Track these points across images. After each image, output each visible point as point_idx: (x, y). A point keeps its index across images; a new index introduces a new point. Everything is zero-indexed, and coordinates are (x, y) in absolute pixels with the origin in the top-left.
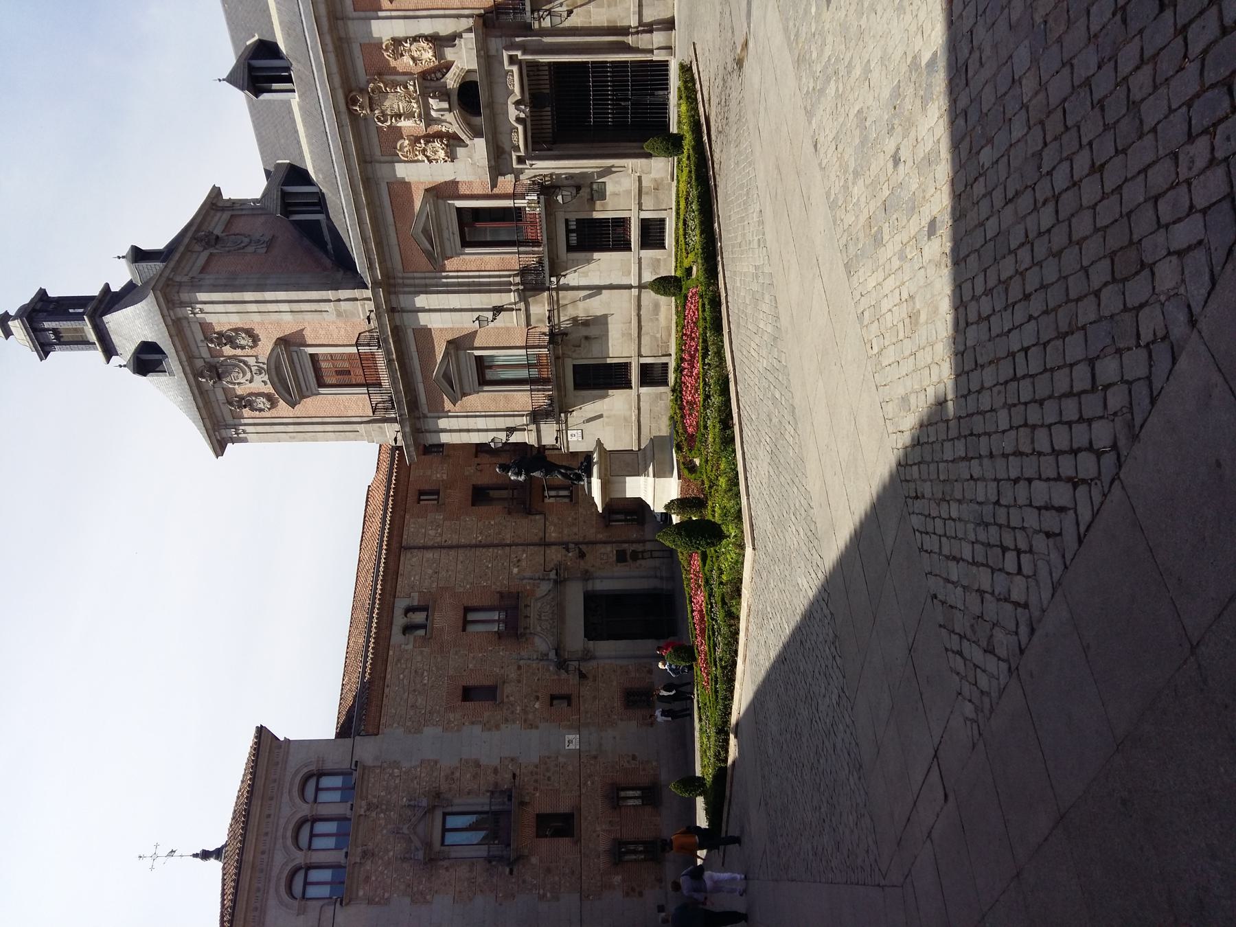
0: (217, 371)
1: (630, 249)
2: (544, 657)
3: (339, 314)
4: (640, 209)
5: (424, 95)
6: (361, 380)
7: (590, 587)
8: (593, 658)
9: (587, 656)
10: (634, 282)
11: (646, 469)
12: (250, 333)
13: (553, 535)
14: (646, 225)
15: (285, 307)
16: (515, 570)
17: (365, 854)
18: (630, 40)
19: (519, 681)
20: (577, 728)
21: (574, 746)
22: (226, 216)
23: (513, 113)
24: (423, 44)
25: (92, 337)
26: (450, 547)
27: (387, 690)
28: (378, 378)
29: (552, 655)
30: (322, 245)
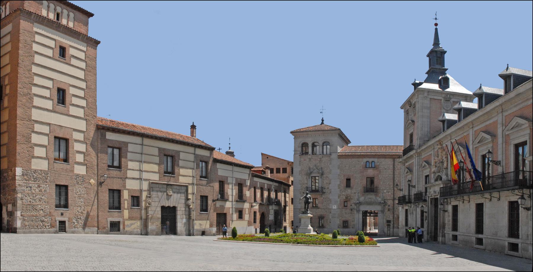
9: (358, 211)
17: (310, 159)
21: (334, 208)
29: (358, 202)
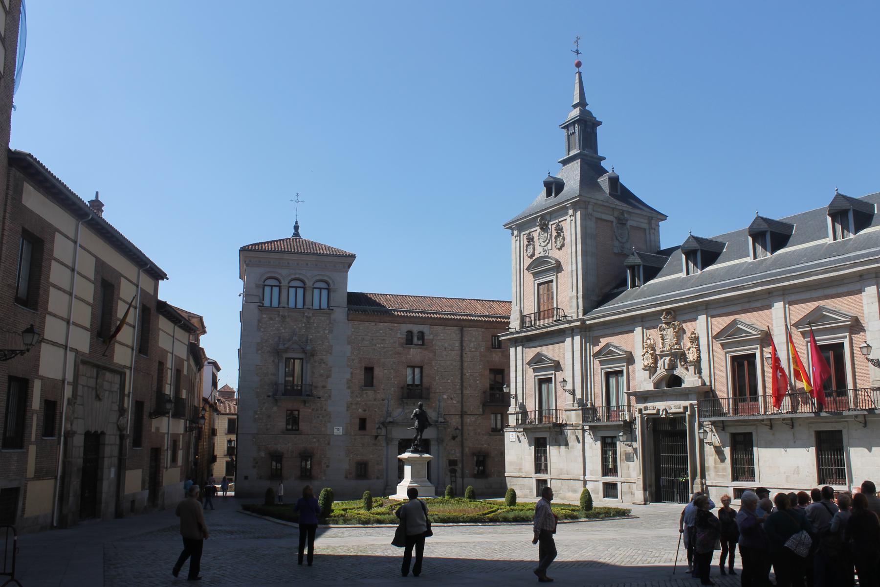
0: (544, 228)
1: (603, 476)
2: (389, 414)
3: (571, 298)
5: (673, 355)
6: (541, 309)
7: (432, 443)
8: (388, 444)
9: (388, 440)
10: (587, 478)
11: (416, 482)
12: (563, 245)
13: (468, 420)
14: (614, 486)
15: (574, 268)
16: (445, 397)
17: (284, 317)
18: (698, 480)
19: (375, 400)
20: (346, 433)
21: (336, 432)
22: (645, 226)
24: (695, 357)
25: (572, 154)
26: (462, 356)
27: (373, 324)
28: (543, 319)
30: (617, 287)
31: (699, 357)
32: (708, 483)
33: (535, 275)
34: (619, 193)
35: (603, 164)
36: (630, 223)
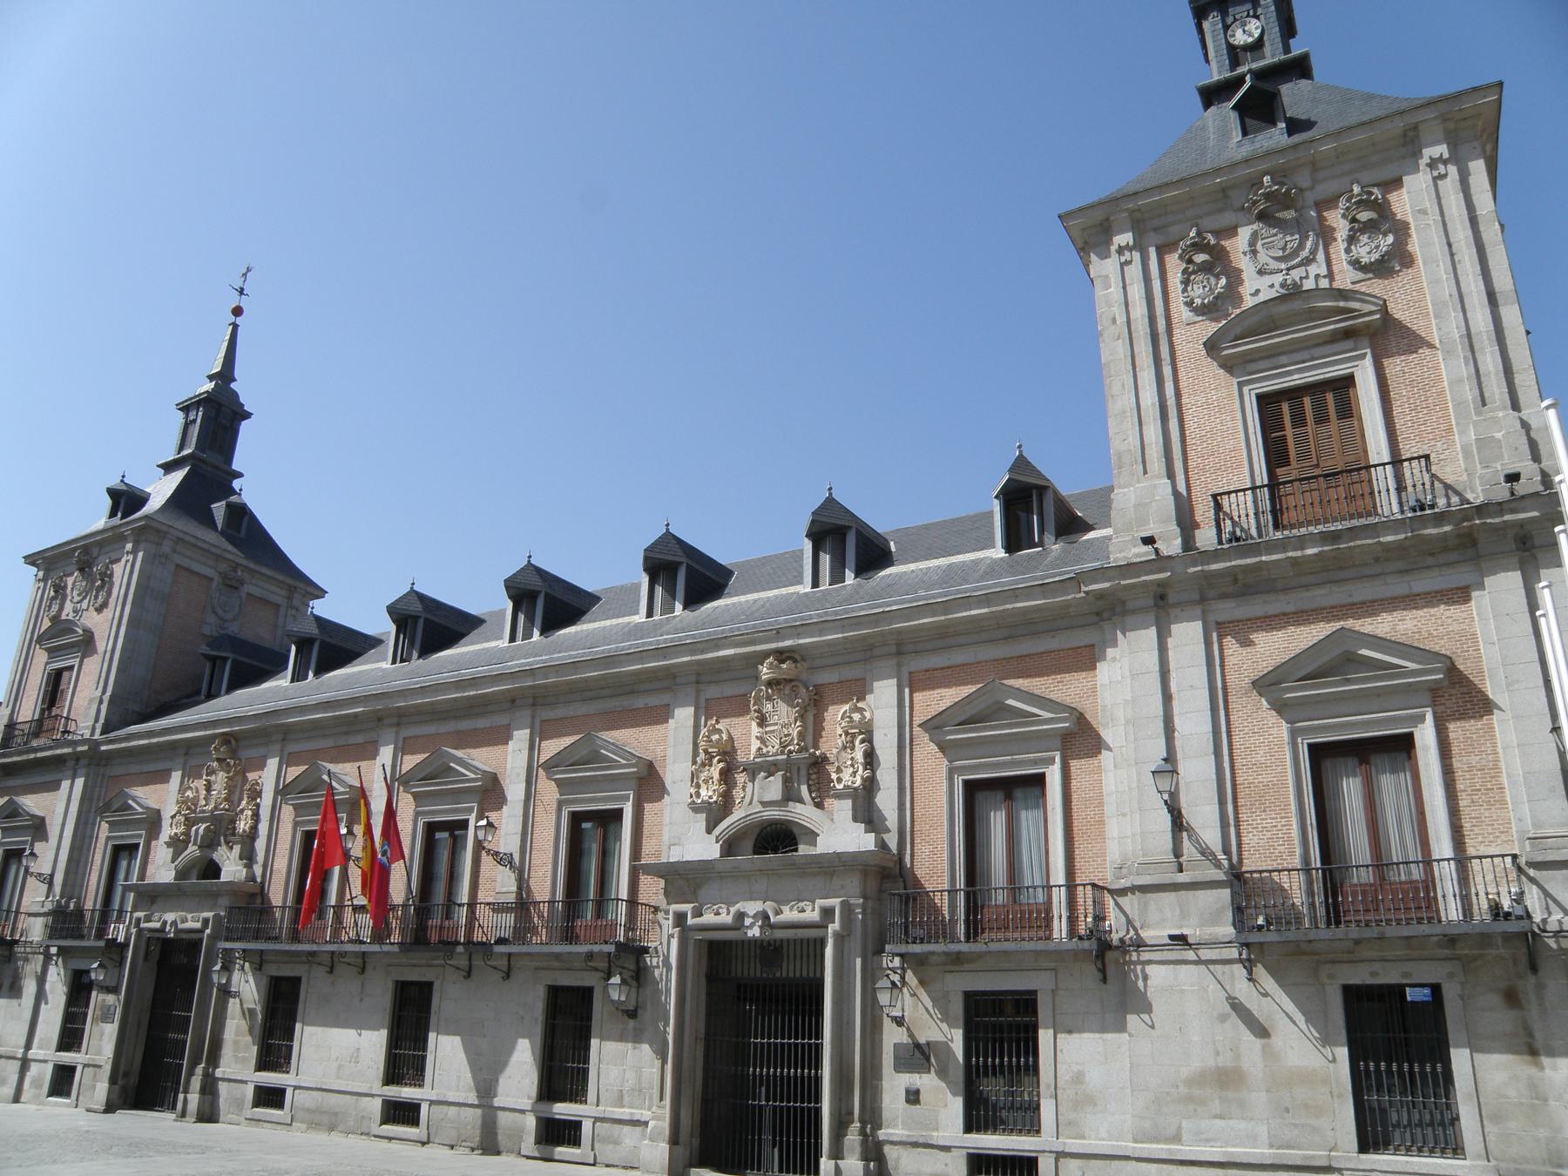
0: (84, 568)
4: (85, 1066)
12: (104, 605)
23: (170, 917)
30: (189, 696)
31: (254, 828)
32: (219, 1073)
33: (53, 652)
34: (243, 534)
35: (236, 484)
36: (247, 588)
